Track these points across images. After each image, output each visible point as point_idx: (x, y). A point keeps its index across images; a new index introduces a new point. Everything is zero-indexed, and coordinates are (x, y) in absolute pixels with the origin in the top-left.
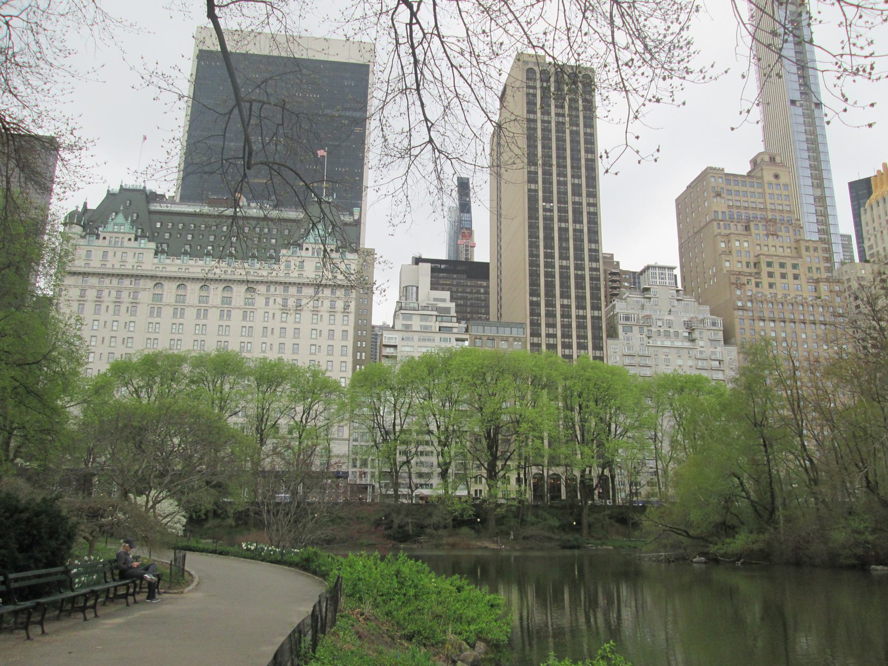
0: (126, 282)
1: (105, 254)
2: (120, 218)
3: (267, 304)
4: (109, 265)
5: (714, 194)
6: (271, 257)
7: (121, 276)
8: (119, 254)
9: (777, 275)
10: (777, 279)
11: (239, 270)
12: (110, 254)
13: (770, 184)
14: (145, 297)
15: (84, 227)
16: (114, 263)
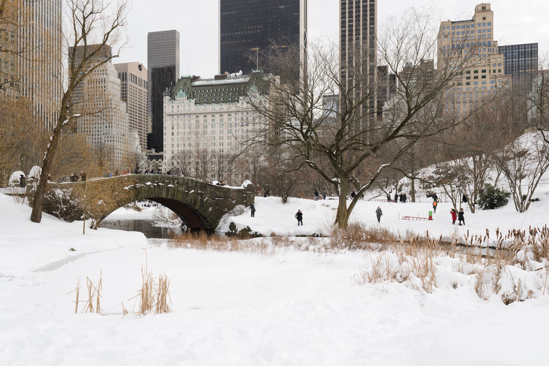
0: (186, 116)
1: (178, 107)
2: (181, 91)
3: (236, 120)
4: (180, 111)
5: (444, 37)
6: (236, 101)
7: (184, 114)
8: (183, 106)
9: (472, 78)
10: (472, 80)
11: (225, 107)
12: (180, 106)
13: (479, 25)
14: (193, 121)
15: (170, 96)
16: (181, 109)
